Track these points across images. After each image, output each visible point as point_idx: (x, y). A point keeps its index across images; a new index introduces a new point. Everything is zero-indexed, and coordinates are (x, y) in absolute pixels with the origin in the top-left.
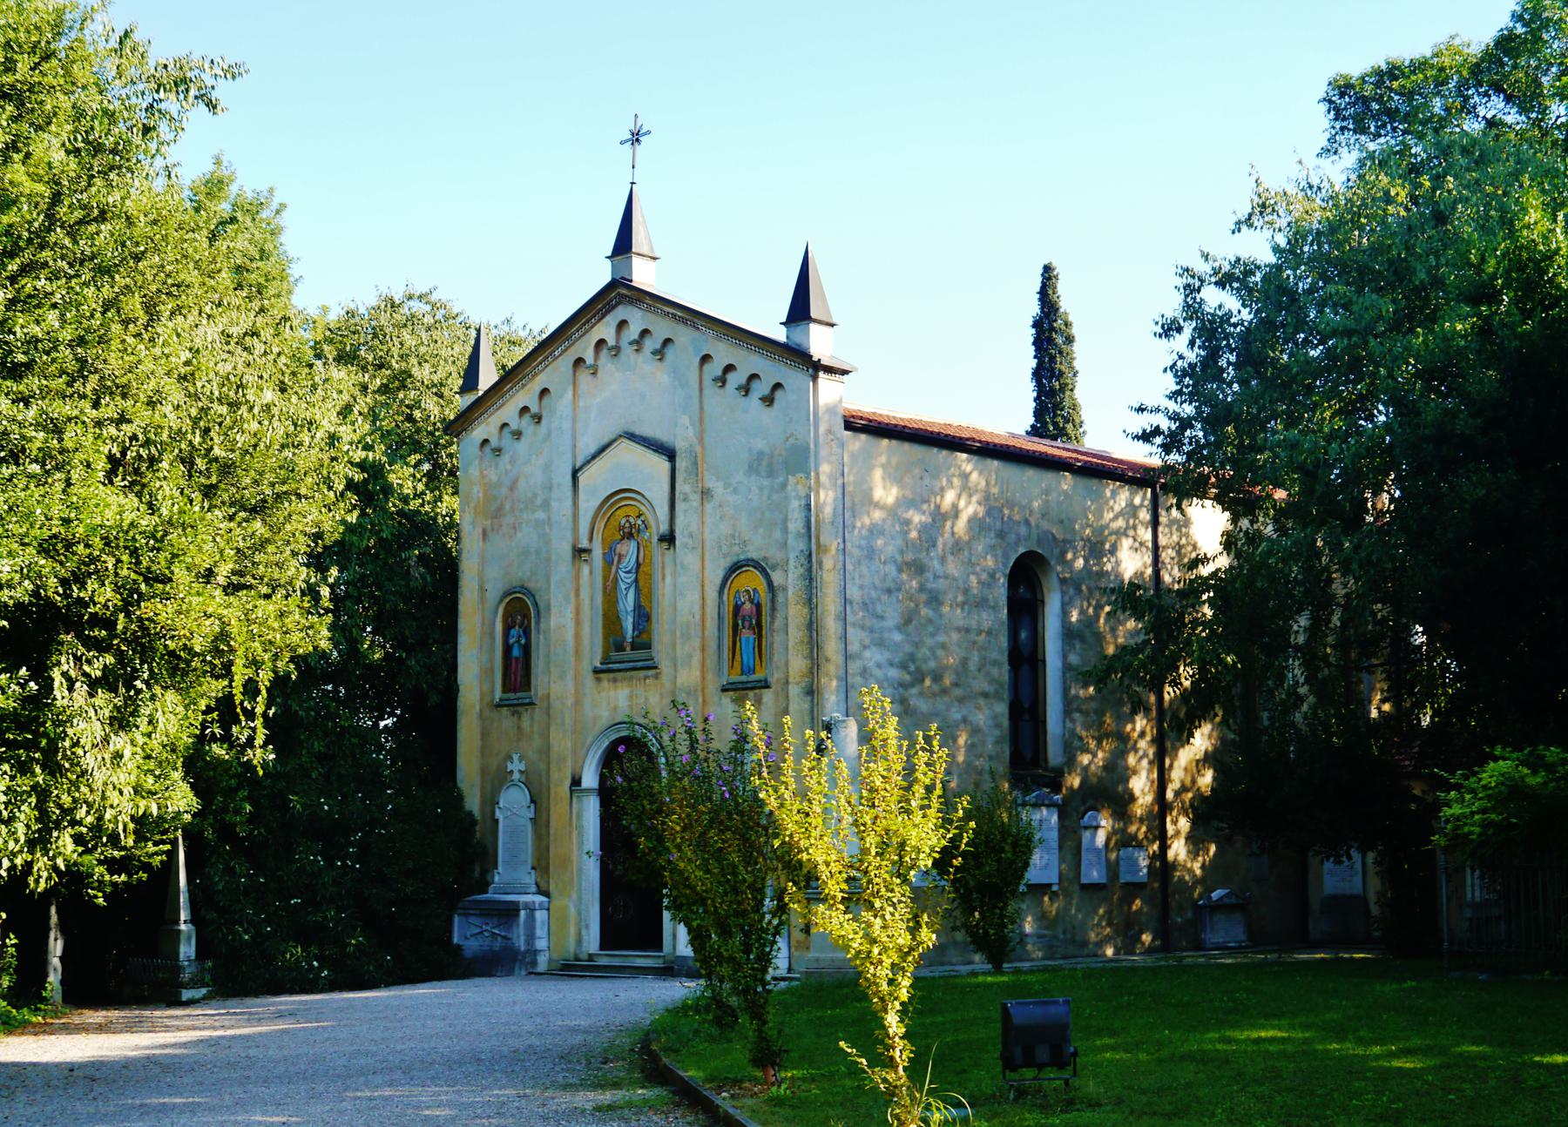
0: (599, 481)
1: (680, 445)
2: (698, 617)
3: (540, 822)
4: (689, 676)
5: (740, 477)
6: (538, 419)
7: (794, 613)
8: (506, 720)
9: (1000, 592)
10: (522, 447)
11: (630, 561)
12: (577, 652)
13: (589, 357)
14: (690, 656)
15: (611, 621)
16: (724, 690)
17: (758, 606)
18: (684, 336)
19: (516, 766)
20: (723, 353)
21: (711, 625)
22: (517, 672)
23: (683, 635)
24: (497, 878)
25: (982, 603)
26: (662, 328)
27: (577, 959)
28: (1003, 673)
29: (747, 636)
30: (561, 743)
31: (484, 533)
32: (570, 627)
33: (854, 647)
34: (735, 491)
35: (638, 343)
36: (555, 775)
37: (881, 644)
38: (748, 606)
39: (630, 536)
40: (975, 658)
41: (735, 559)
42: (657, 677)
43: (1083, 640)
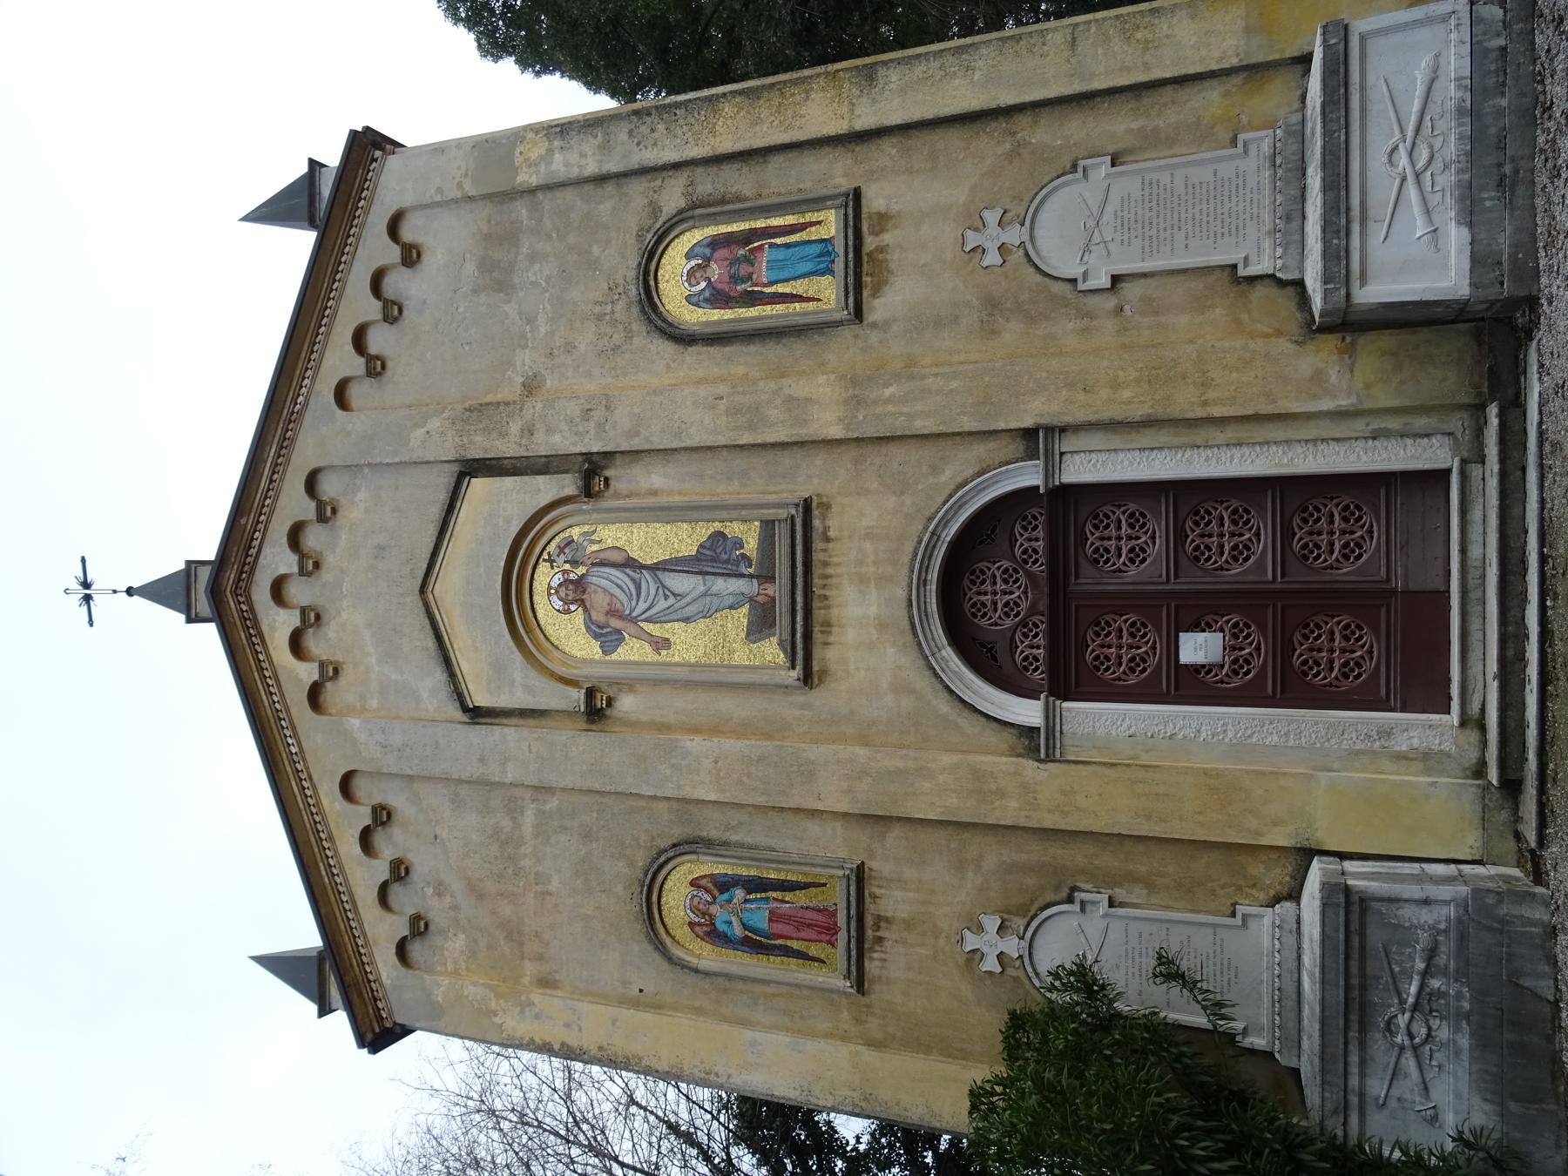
2: (722, 389)
5: (511, 309)
8: (893, 963)
10: (423, 863)
13: (307, 673)
14: (790, 399)
16: (859, 314)
17: (715, 243)
18: (306, 452)
19: (991, 944)
20: (338, 359)
23: (751, 427)
24: (1259, 1042)
26: (292, 503)
27: (1479, 771)
31: (546, 983)
34: (531, 320)
36: (1009, 811)
38: (715, 271)
39: (580, 584)
41: (635, 310)
42: (826, 506)
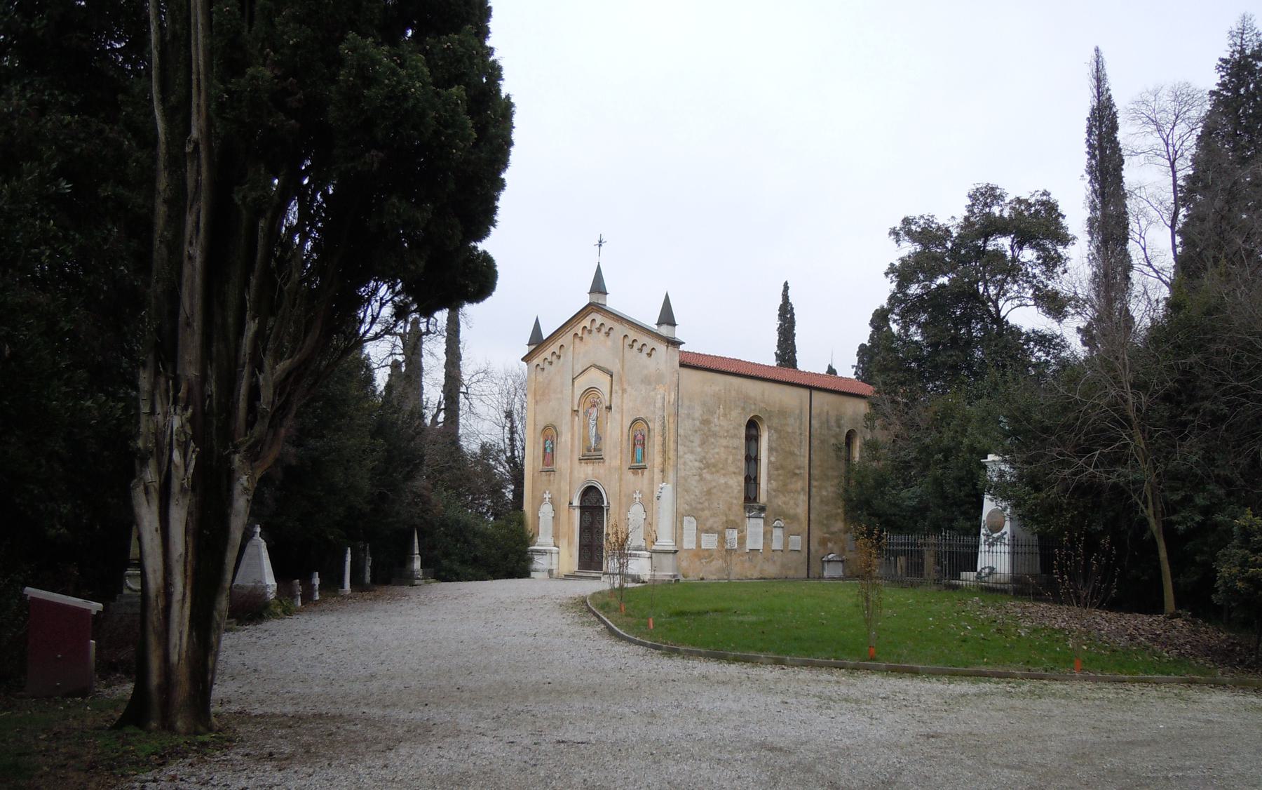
0: (583, 383)
1: (615, 371)
3: (556, 518)
4: (616, 463)
6: (559, 357)
7: (657, 440)
8: (544, 477)
9: (743, 432)
10: (552, 368)
11: (594, 416)
12: (572, 451)
15: (586, 439)
18: (617, 327)
19: (547, 496)
20: (633, 334)
21: (625, 443)
22: (549, 456)
25: (734, 436)
26: (609, 323)
28: (743, 464)
29: (639, 448)
30: (565, 487)
32: (569, 442)
33: (681, 453)
35: (599, 330)
37: (692, 452)
40: (731, 458)
43: (777, 451)
